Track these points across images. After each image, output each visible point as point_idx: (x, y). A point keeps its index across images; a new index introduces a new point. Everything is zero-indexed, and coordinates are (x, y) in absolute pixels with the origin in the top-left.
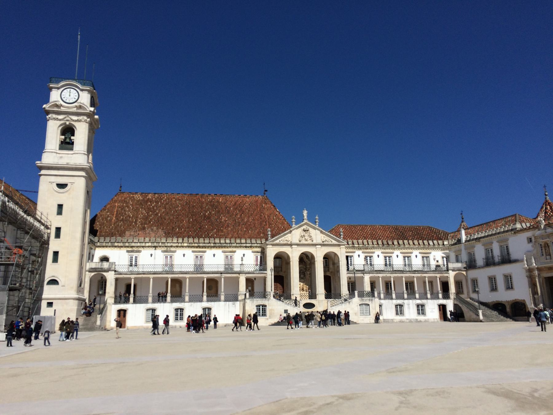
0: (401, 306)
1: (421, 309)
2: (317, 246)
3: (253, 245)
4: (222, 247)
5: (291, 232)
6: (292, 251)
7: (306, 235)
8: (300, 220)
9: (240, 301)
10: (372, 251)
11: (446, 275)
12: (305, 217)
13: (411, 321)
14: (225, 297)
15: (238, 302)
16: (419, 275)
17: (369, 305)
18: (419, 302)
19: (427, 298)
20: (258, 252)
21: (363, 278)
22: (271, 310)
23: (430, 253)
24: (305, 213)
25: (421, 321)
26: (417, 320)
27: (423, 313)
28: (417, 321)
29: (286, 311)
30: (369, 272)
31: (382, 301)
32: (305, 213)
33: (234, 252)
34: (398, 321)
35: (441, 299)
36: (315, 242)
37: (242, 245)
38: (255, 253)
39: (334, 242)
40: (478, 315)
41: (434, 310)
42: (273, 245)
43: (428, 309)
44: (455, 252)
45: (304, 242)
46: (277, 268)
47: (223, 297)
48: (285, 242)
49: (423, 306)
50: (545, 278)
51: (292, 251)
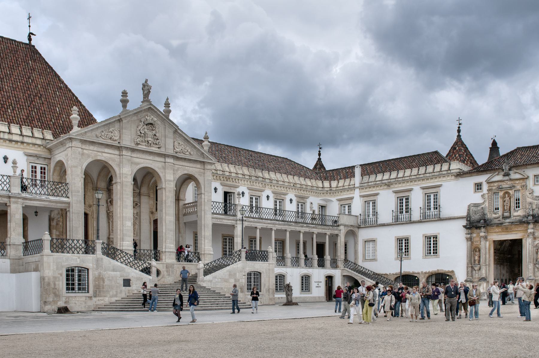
2: (169, 160)
7: (150, 133)
10: (234, 183)
11: (336, 232)
23: (307, 198)
36: (162, 151)
43: (313, 285)
48: (109, 142)
50: (494, 241)
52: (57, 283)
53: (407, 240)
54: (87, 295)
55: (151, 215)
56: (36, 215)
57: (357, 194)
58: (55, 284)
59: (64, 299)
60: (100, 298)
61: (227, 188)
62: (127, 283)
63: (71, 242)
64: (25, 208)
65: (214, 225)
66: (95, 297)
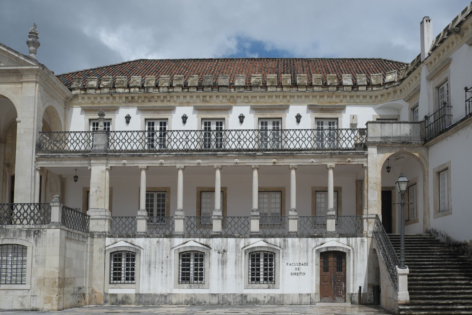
0: (200, 257)
1: (262, 266)
13: (223, 302)
16: (269, 162)
17: (24, 248)
18: (257, 243)
19: (290, 235)
25: (256, 302)
26: (244, 296)
27: (270, 278)
28: (244, 301)
30: (107, 154)
31: (139, 242)
34: (182, 299)
35: (332, 235)
40: (396, 288)
41: (303, 269)
43: (284, 269)
44: (408, 100)
49: (270, 256)
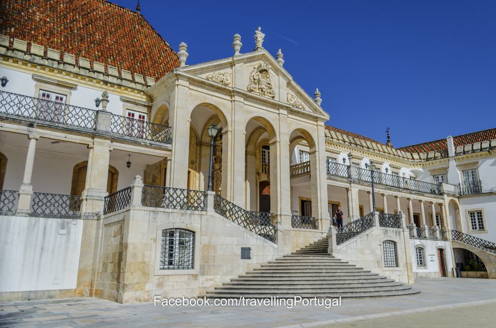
2: (282, 111)
3: (124, 83)
4: (34, 65)
5: (232, 65)
6: (233, 109)
8: (249, 46)
9: (87, 218)
12: (260, 44)
14: (34, 203)
15: (80, 222)
20: (136, 103)
21: (347, 189)
22: (207, 247)
24: (260, 36)
29: (246, 253)
32: (260, 36)
33: (72, 87)
37: (95, 75)
38: (129, 105)
39: (308, 110)
42: (192, 81)
45: (256, 94)
46: (197, 142)
47: (25, 202)
51: (233, 109)
52: (147, 253)
53: (480, 213)
54: (191, 271)
55: (257, 176)
56: (129, 167)
57: (453, 164)
58: (143, 256)
59: (155, 280)
60: (209, 277)
61: (329, 153)
62: (246, 253)
63: (171, 191)
64: (113, 154)
65: (329, 186)
66: (203, 274)
